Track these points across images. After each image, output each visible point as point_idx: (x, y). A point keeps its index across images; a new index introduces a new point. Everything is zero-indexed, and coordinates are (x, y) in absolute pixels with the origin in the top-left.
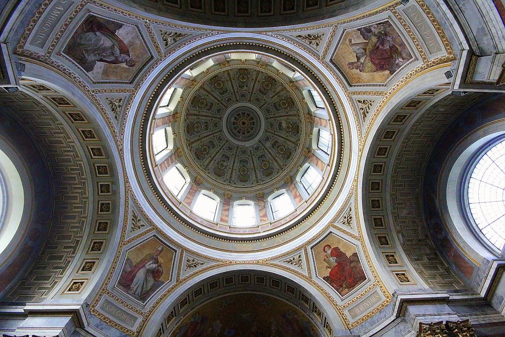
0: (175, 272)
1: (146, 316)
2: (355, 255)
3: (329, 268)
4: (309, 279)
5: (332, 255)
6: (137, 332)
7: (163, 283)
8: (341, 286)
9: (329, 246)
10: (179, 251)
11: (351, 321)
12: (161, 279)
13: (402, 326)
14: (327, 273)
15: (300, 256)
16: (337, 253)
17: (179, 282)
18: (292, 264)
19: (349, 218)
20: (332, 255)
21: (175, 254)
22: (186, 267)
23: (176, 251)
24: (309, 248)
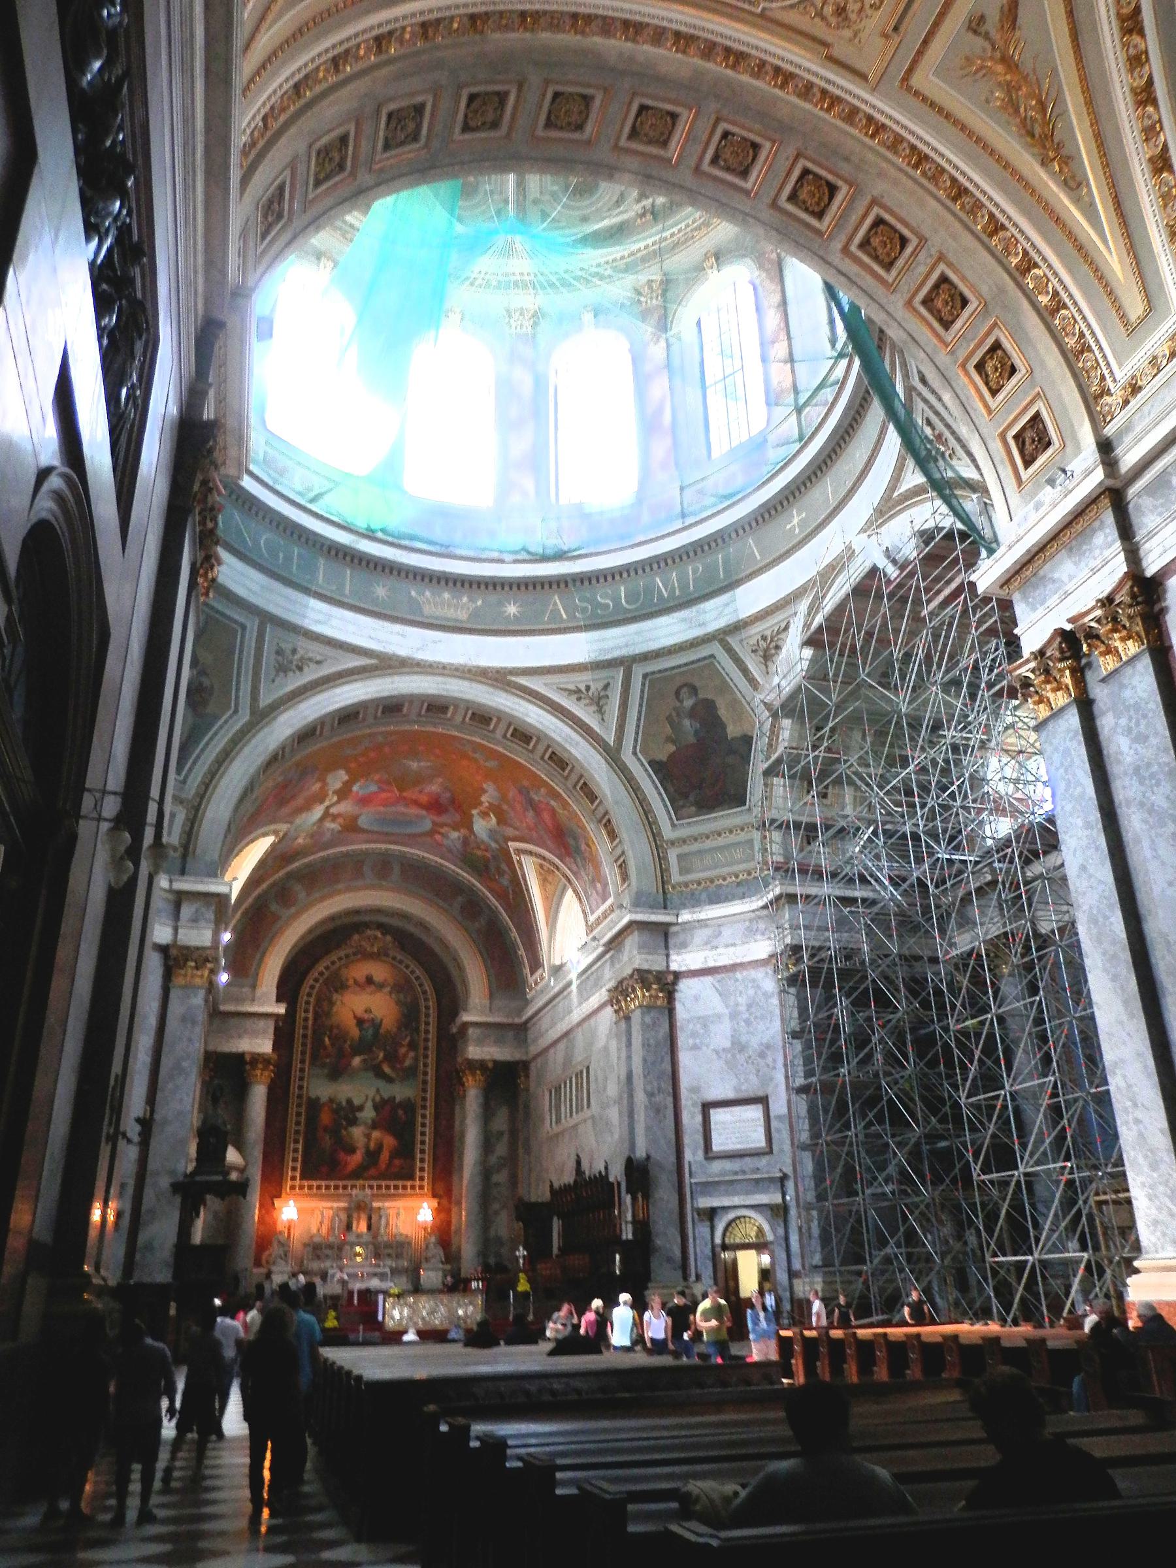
0: (246, 687)
1: (193, 807)
2: (747, 740)
3: (673, 742)
4: (612, 755)
5: (692, 713)
6: (181, 845)
7: (216, 718)
8: (686, 796)
9: (694, 690)
10: (252, 625)
11: (676, 877)
12: (211, 708)
13: (762, 926)
14: (664, 752)
15: (606, 687)
16: (707, 714)
17: (262, 716)
18: (579, 699)
19: (773, 644)
20: (692, 713)
21: (243, 636)
22: (273, 673)
23: (244, 627)
24: (638, 672)
